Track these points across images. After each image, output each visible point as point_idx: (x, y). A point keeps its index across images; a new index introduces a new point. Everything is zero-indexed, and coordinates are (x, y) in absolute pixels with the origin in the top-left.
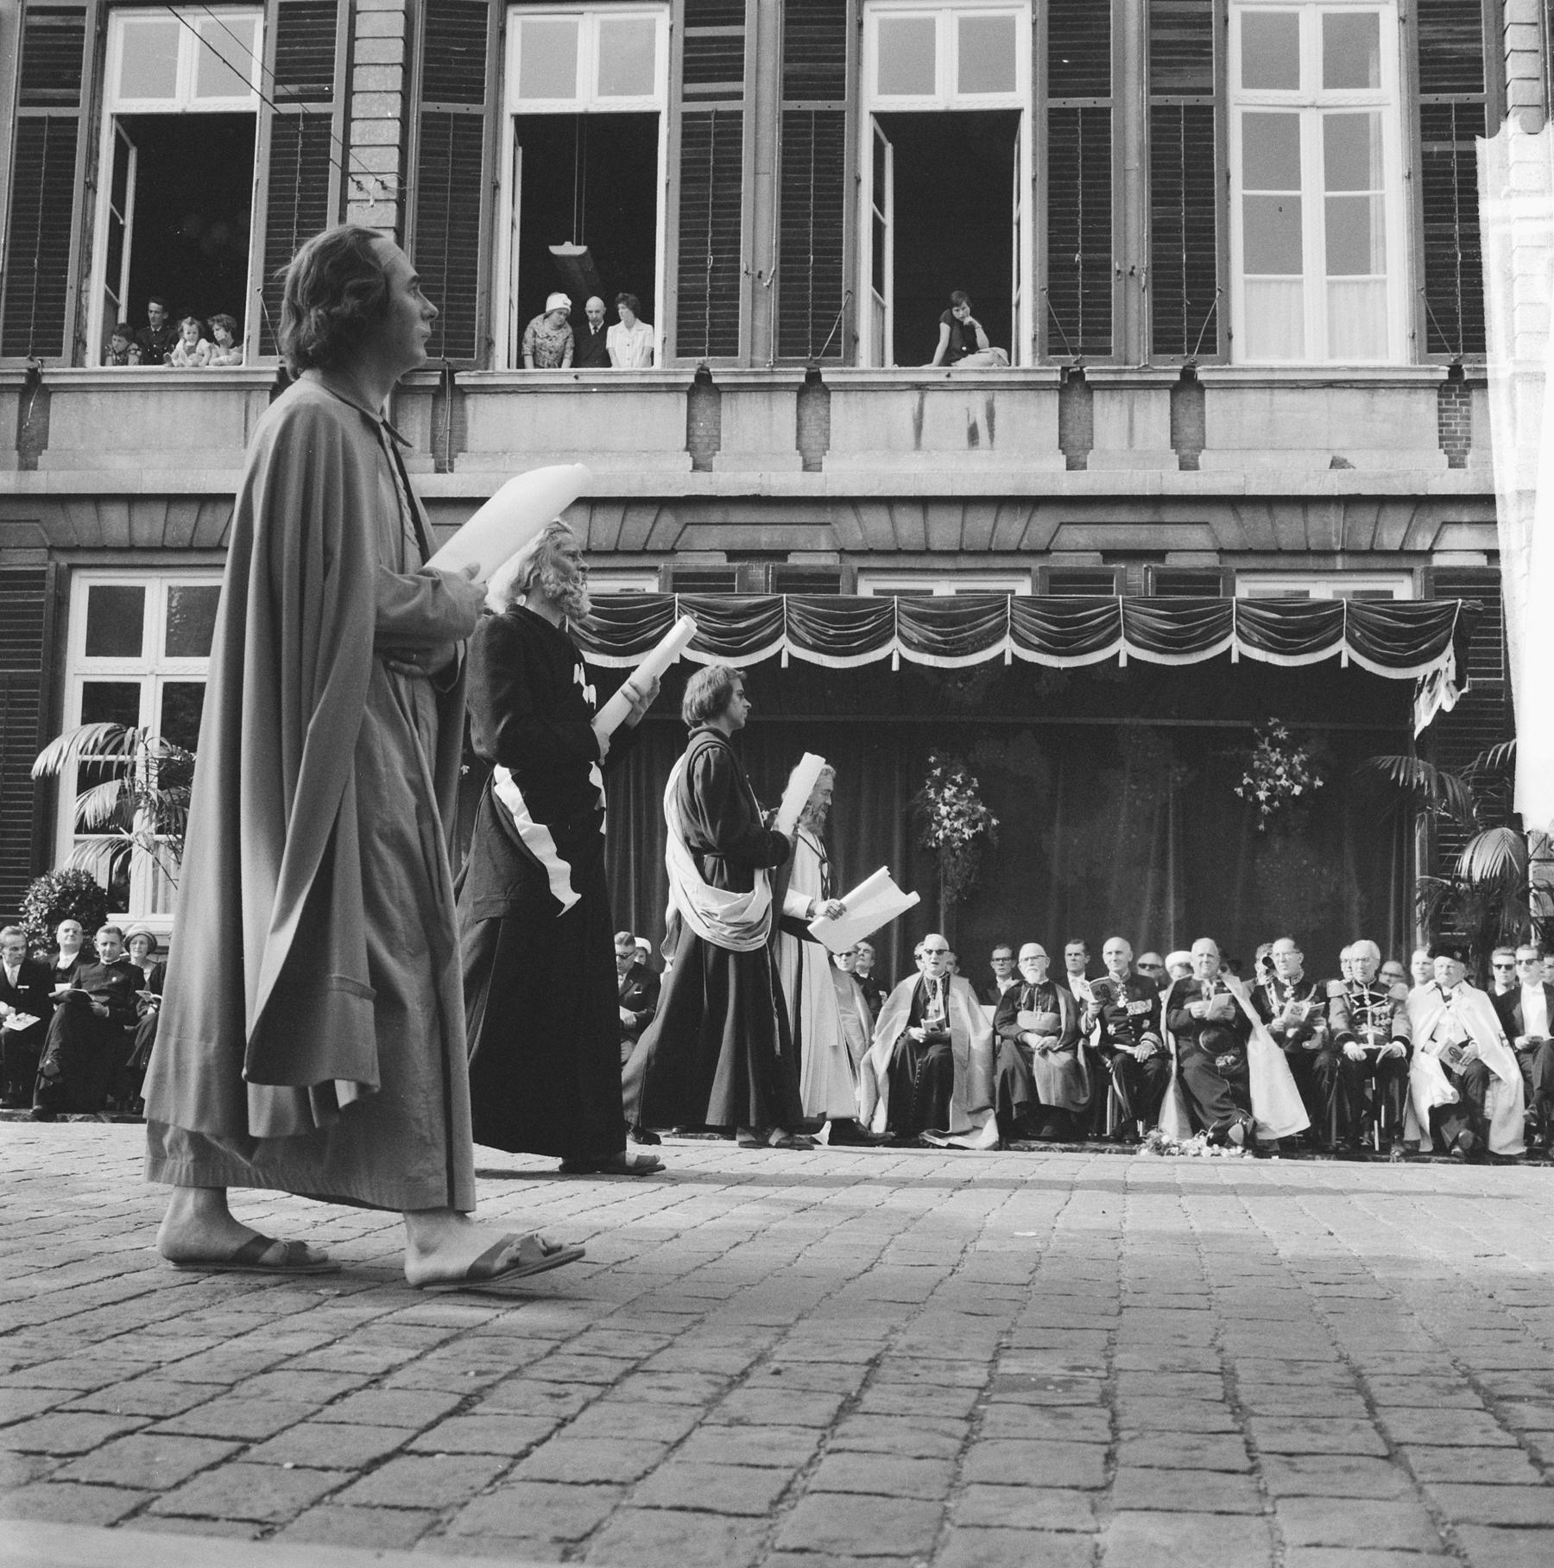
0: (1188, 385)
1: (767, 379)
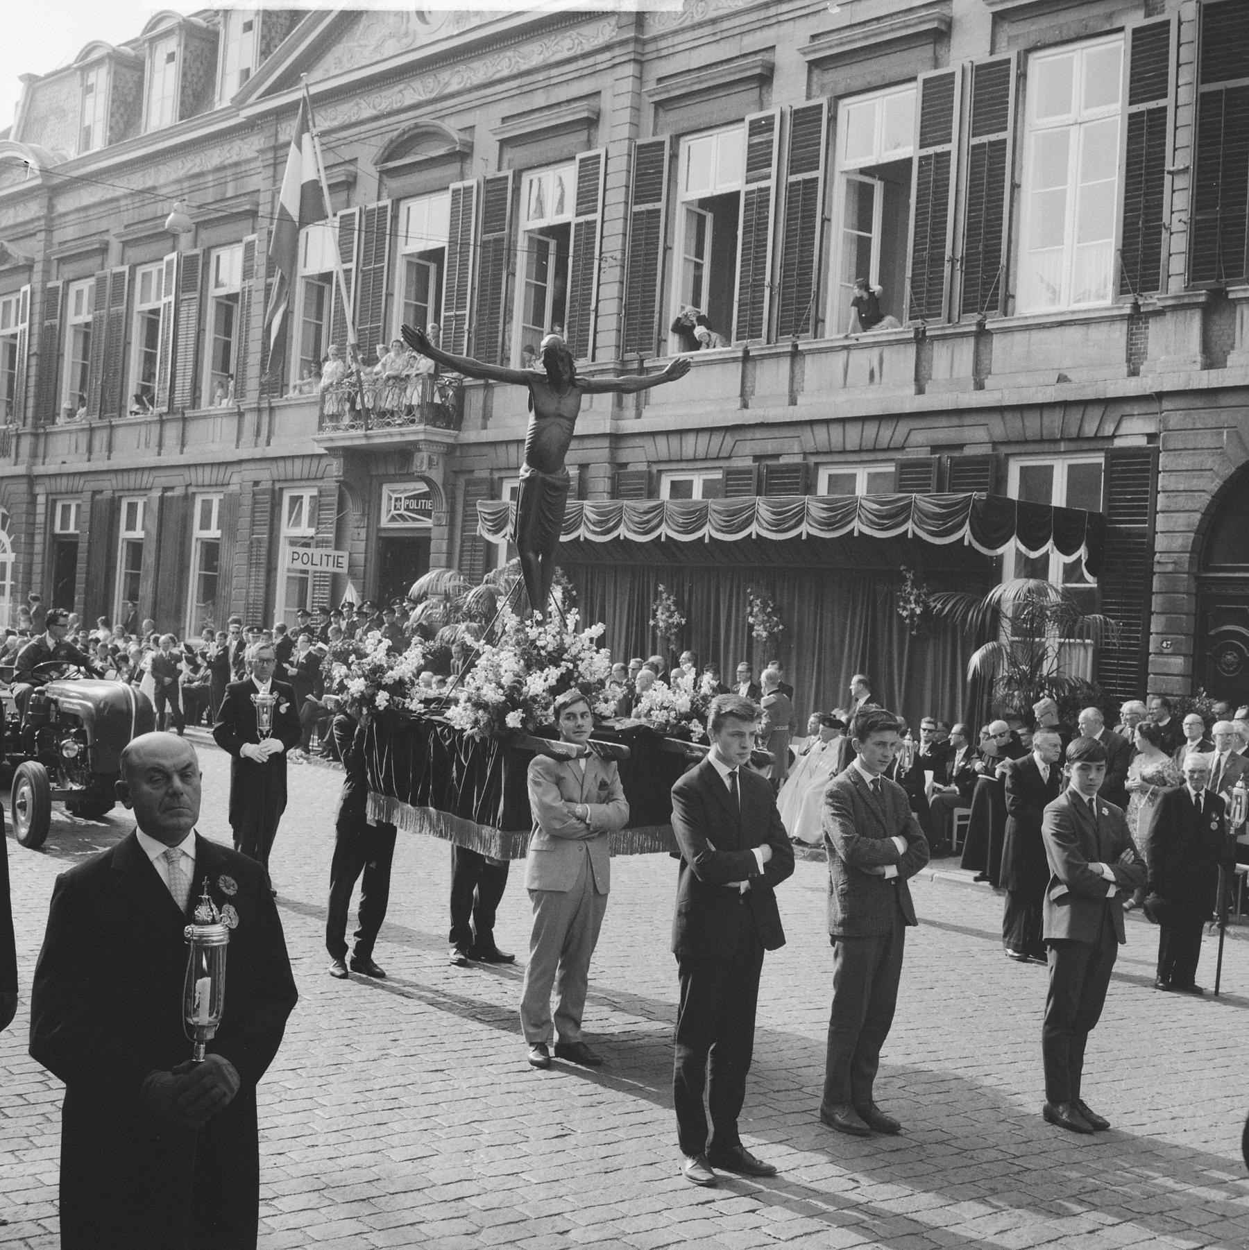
0: (982, 334)
1: (774, 351)
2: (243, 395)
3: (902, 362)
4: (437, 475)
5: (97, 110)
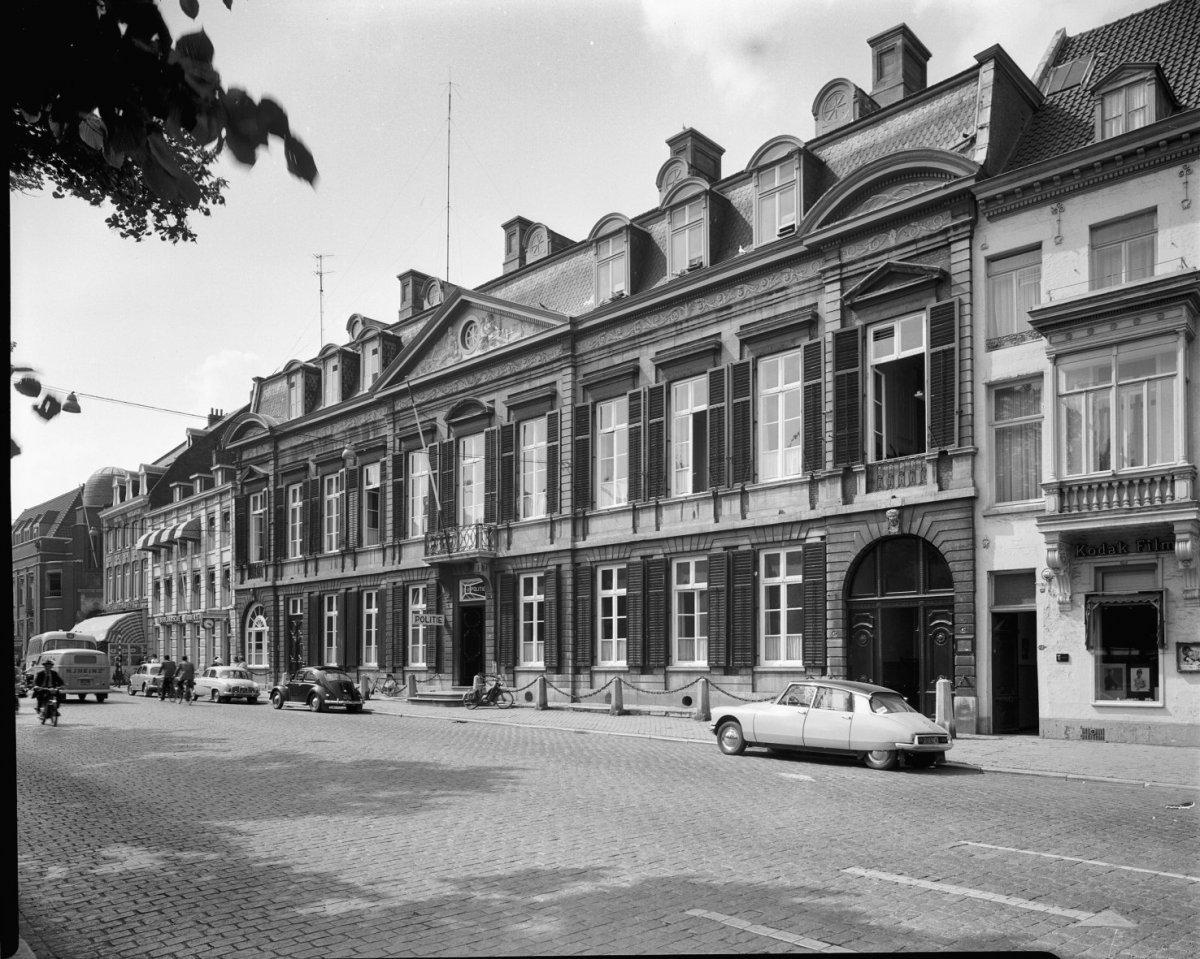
0: (744, 494)
2: (385, 540)
3: (708, 509)
4: (486, 574)
5: (298, 395)
